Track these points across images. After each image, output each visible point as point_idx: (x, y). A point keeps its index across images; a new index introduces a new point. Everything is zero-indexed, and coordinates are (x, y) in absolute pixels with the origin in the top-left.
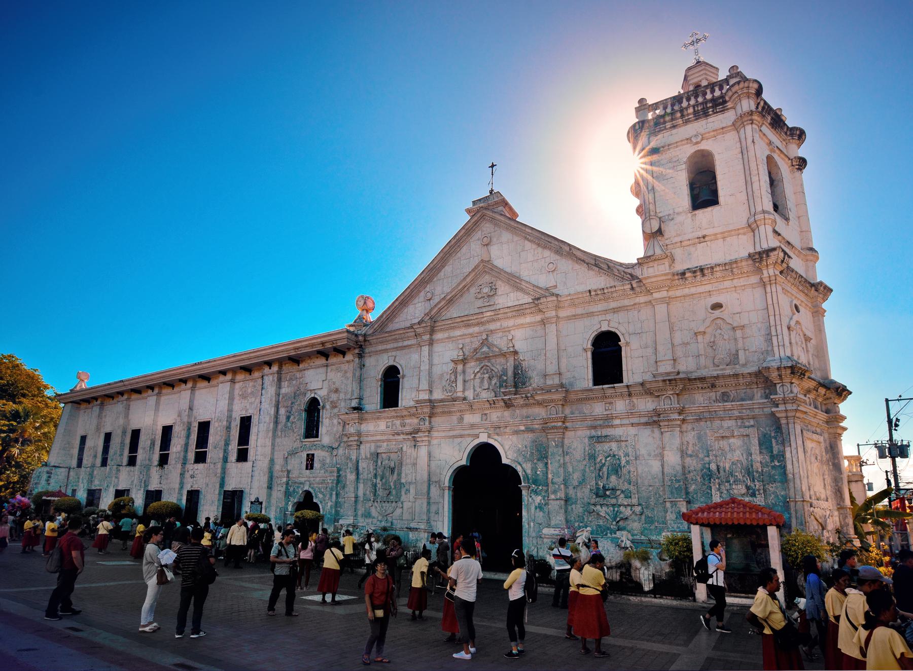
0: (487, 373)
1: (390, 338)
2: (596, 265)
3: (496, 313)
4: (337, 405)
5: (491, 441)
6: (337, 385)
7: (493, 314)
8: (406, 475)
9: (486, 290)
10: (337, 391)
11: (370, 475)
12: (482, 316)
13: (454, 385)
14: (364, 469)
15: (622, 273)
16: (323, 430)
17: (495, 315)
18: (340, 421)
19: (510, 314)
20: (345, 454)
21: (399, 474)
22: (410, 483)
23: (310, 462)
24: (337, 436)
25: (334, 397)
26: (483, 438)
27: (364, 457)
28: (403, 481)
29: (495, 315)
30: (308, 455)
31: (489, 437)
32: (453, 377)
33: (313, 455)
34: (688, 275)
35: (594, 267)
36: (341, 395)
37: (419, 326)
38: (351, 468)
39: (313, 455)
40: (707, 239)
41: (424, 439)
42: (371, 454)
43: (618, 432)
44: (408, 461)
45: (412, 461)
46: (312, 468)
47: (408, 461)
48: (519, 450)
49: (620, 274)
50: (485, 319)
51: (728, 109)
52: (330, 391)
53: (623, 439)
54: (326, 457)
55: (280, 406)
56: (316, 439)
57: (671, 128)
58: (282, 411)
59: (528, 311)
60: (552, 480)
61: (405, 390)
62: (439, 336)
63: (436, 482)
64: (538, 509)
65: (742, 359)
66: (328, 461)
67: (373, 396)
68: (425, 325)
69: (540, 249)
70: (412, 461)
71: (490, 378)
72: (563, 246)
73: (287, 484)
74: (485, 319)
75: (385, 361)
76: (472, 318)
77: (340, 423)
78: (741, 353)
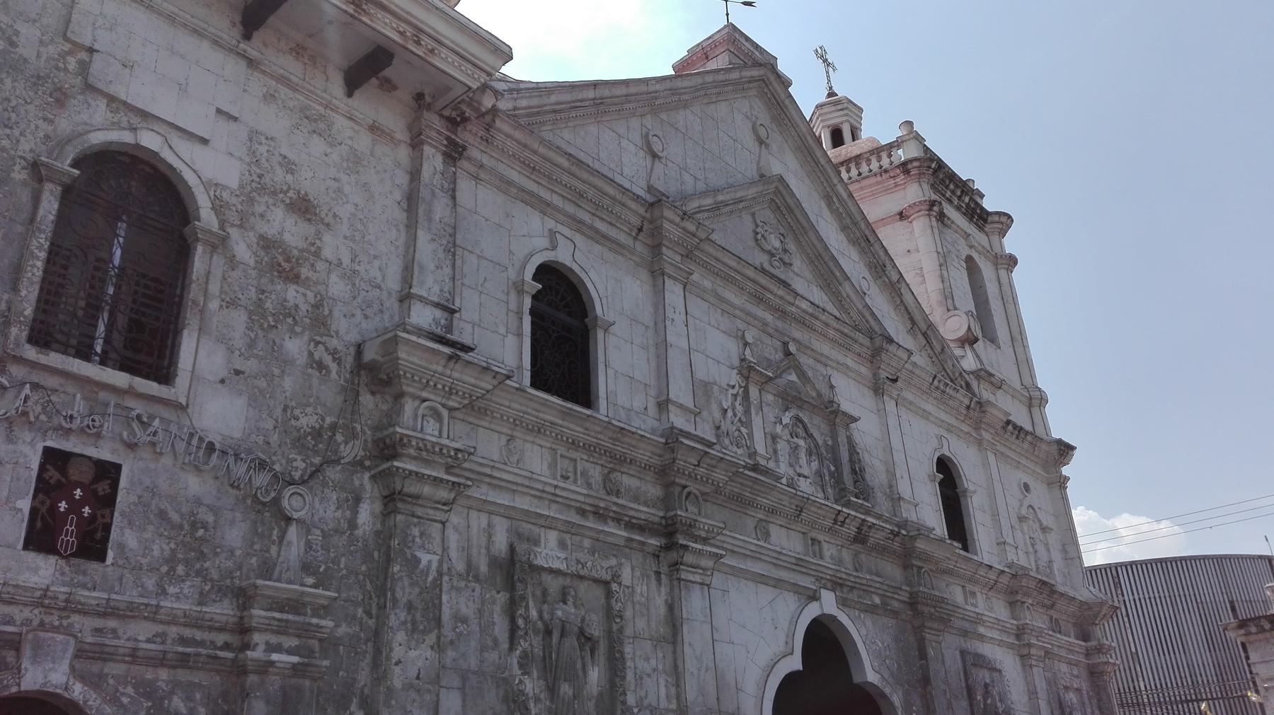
1: (566, 178)
2: (925, 335)
4: (305, 272)
5: (843, 618)
6: (310, 182)
7: (810, 310)
8: (639, 679)
10: (303, 207)
11: (492, 656)
12: (791, 300)
14: (464, 620)
15: (957, 374)
17: (812, 315)
18: (320, 353)
20: (353, 525)
24: (307, 421)
26: (828, 603)
27: (460, 567)
28: (631, 699)
30: (52, 457)
32: (739, 409)
33: (108, 472)
34: (1010, 427)
35: (920, 336)
36: (327, 238)
37: (677, 220)
38: (410, 607)
39: (108, 472)
42: (494, 562)
43: (987, 650)
44: (641, 624)
45: (653, 624)
47: (641, 624)
49: (954, 373)
50: (794, 309)
51: (983, 230)
53: (998, 667)
54: (215, 510)
56: (152, 387)
59: (857, 348)
68: (692, 228)
70: (653, 624)
71: (810, 453)
72: (889, 268)
74: (794, 309)
77: (320, 366)
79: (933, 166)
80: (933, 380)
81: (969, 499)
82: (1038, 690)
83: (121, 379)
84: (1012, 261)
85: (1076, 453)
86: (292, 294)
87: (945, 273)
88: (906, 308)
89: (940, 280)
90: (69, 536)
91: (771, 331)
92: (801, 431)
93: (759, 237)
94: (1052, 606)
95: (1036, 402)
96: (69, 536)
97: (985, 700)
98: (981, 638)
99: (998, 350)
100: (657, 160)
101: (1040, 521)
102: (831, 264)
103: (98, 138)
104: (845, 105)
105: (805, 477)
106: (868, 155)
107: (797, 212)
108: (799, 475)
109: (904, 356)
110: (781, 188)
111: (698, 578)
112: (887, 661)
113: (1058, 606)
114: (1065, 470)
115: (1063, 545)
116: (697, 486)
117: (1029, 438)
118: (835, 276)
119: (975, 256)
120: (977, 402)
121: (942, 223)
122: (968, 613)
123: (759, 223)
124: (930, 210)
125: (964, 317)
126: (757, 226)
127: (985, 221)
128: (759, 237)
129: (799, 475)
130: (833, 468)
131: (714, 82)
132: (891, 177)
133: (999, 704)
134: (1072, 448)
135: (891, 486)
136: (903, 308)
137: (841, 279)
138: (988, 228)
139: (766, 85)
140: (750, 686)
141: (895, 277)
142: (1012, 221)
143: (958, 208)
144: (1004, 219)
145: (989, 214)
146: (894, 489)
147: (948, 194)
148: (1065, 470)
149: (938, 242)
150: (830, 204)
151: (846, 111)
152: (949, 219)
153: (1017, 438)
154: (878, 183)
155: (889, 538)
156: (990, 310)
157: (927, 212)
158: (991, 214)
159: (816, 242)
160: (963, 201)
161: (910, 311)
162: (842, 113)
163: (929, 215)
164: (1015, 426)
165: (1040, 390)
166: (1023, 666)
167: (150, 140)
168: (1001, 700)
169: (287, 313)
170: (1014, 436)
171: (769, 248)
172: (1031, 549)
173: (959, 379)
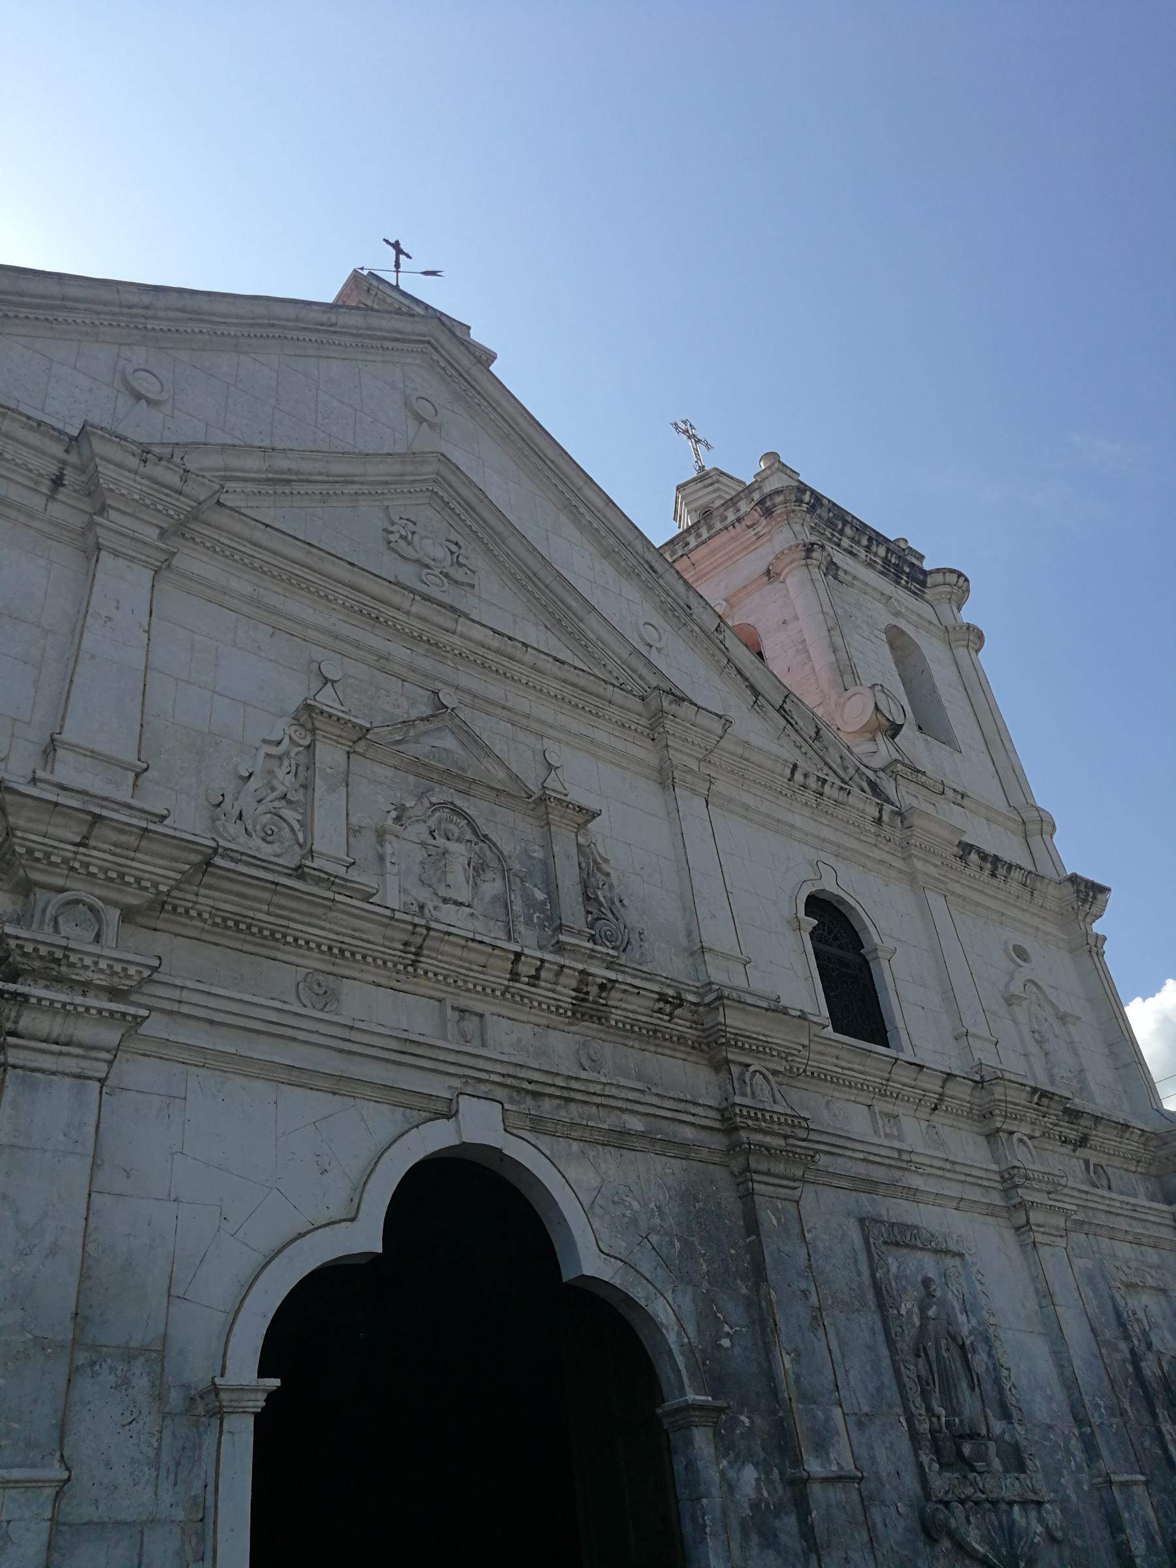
0: (459, 840)
2: (781, 710)
3: (510, 650)
12: (450, 625)
15: (852, 771)
17: (497, 652)
19: (553, 686)
29: (497, 652)
34: (974, 857)
37: (133, 462)
40: (966, 802)
41: (84, 1031)
48: (634, 1221)
49: (845, 769)
50: (456, 640)
51: (922, 598)
53: (953, 1247)
57: (845, 550)
60: (798, 1377)
63: (129, 1355)
64: (755, 1539)
68: (173, 479)
74: (456, 640)
76: (406, 605)
79: (807, 497)
80: (793, 773)
81: (884, 964)
82: (1056, 1288)
84: (974, 637)
85: (1112, 897)
87: (838, 640)
88: (739, 672)
89: (830, 651)
91: (404, 672)
92: (458, 827)
93: (393, 538)
94: (1083, 1141)
95: (1033, 828)
97: (923, 1309)
98: (913, 1194)
99: (957, 755)
100: (143, 402)
101: (1053, 1005)
102: (558, 588)
104: (715, 478)
105: (456, 903)
106: (722, 509)
107: (481, 509)
108: (445, 901)
109: (717, 727)
110: (446, 473)
111: (70, 1065)
112: (654, 1238)
113: (1095, 1141)
114: (1098, 927)
115: (1110, 1046)
116: (98, 891)
117: (1015, 874)
118: (569, 608)
120: (894, 813)
121: (835, 577)
122: (875, 1150)
123: (396, 518)
124: (808, 557)
125: (868, 692)
126: (393, 523)
127: (923, 584)
128: (393, 538)
129: (445, 901)
130: (540, 896)
131: (297, 319)
132: (749, 527)
133: (962, 1318)
134: (1104, 890)
135: (689, 934)
136: (734, 672)
137: (581, 612)
138: (929, 594)
139: (435, 349)
141: (711, 624)
142: (966, 580)
143: (870, 565)
144: (952, 578)
145: (925, 573)
146: (695, 935)
147: (846, 543)
148: (1098, 927)
149: (824, 598)
150: (576, 518)
151: (716, 486)
152: (846, 572)
153: (993, 875)
154: (733, 539)
155: (660, 1011)
156: (939, 701)
157: (804, 562)
158: (931, 572)
159: (524, 555)
160: (876, 554)
161: (748, 675)
162: (711, 488)
163: (807, 565)
164: (984, 856)
165: (1038, 809)
166: (1022, 1246)
168: (965, 1311)
170: (987, 872)
171: (415, 555)
172: (1033, 1048)
173: (856, 777)
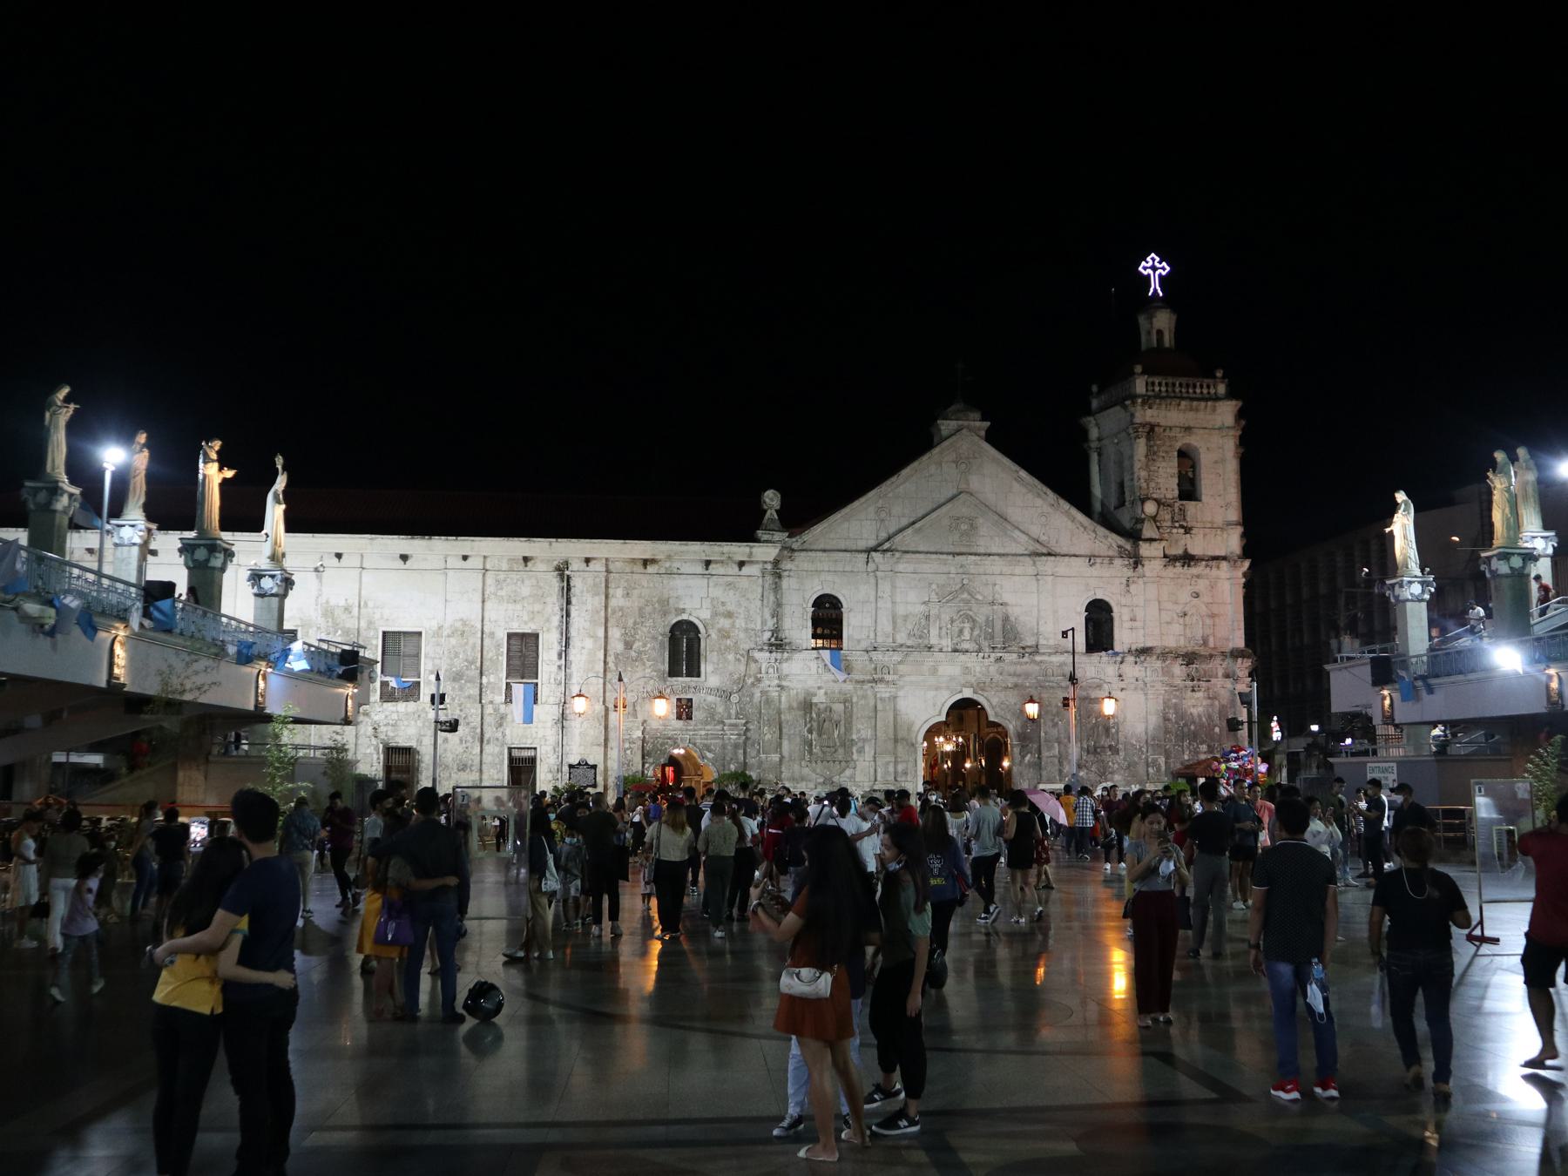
6: (730, 607)
8: (859, 731)
9: (964, 527)
10: (729, 615)
13: (926, 631)
16: (705, 667)
18: (738, 656)
21: (848, 729)
22: (864, 740)
23: (685, 710)
25: (724, 623)
30: (679, 700)
31: (975, 692)
33: (690, 700)
39: (690, 700)
46: (689, 717)
52: (715, 614)
55: (609, 625)
58: (615, 633)
61: (851, 628)
62: (901, 567)
65: (1211, 644)
66: (720, 709)
67: (799, 628)
69: (1030, 496)
73: (644, 741)
75: (816, 589)
77: (739, 660)
78: (1211, 640)
83: (689, 679)
86: (728, 642)
90: (684, 716)
96: (684, 716)
103: (674, 621)
119: (1194, 440)
140: (915, 728)
167: (685, 617)
169: (728, 648)
